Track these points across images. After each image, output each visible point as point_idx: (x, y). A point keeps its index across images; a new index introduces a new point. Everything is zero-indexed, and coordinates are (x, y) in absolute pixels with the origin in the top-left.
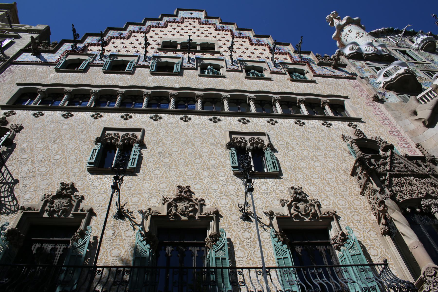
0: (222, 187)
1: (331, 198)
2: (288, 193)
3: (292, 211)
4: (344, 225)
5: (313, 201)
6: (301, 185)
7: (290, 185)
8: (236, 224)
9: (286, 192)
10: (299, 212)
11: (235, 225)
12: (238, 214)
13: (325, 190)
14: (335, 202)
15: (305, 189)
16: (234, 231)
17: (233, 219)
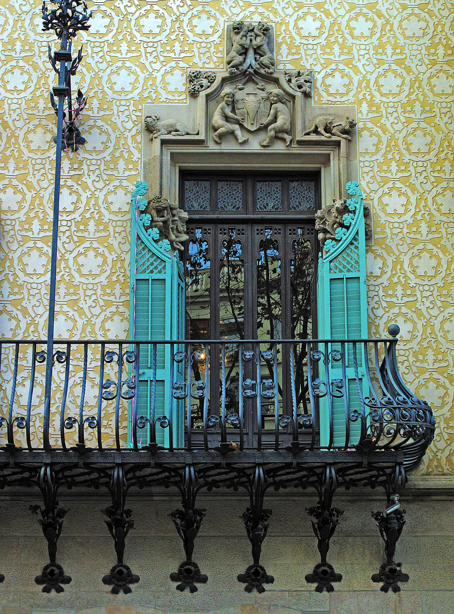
0: (16, 21)
1: (360, 65)
2: (223, 48)
3: (217, 119)
4: (367, 170)
5: (294, 80)
6: (275, 12)
7: (236, 10)
8: (39, 161)
9: (218, 41)
10: (238, 122)
11: (37, 167)
12: (51, 126)
13: (351, 31)
14: (369, 81)
15: (283, 28)
16: (30, 187)
17: (33, 146)
